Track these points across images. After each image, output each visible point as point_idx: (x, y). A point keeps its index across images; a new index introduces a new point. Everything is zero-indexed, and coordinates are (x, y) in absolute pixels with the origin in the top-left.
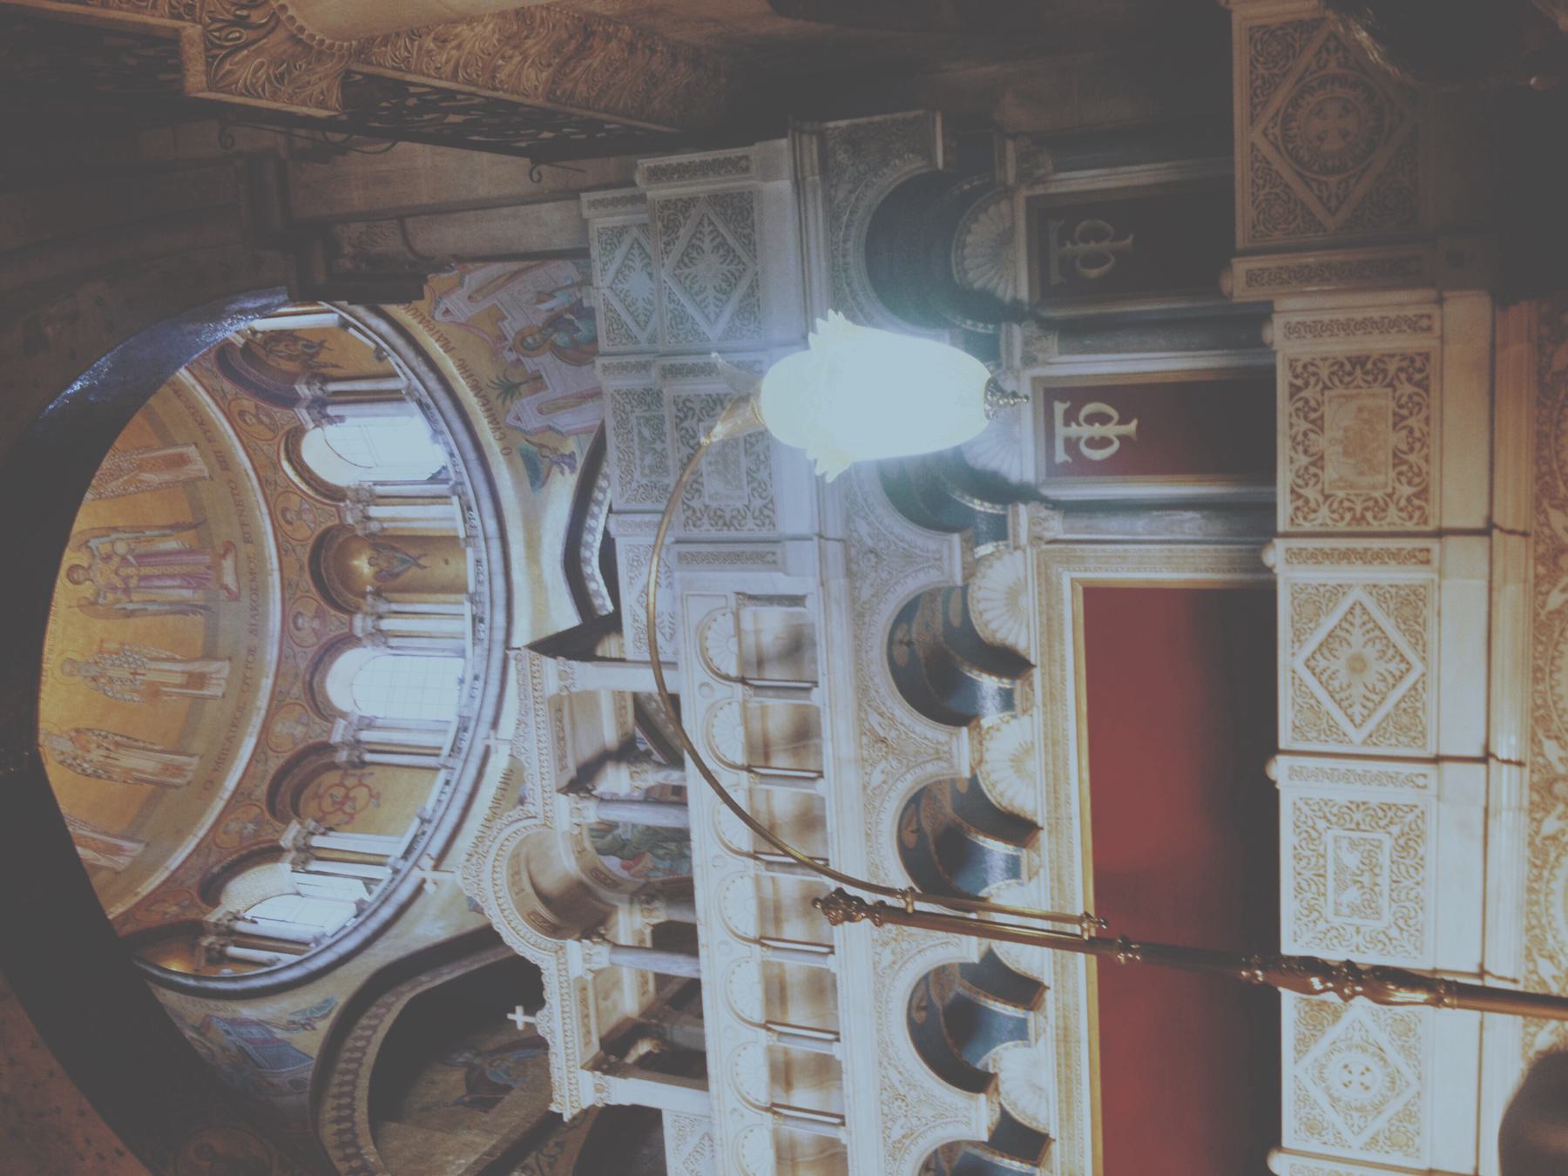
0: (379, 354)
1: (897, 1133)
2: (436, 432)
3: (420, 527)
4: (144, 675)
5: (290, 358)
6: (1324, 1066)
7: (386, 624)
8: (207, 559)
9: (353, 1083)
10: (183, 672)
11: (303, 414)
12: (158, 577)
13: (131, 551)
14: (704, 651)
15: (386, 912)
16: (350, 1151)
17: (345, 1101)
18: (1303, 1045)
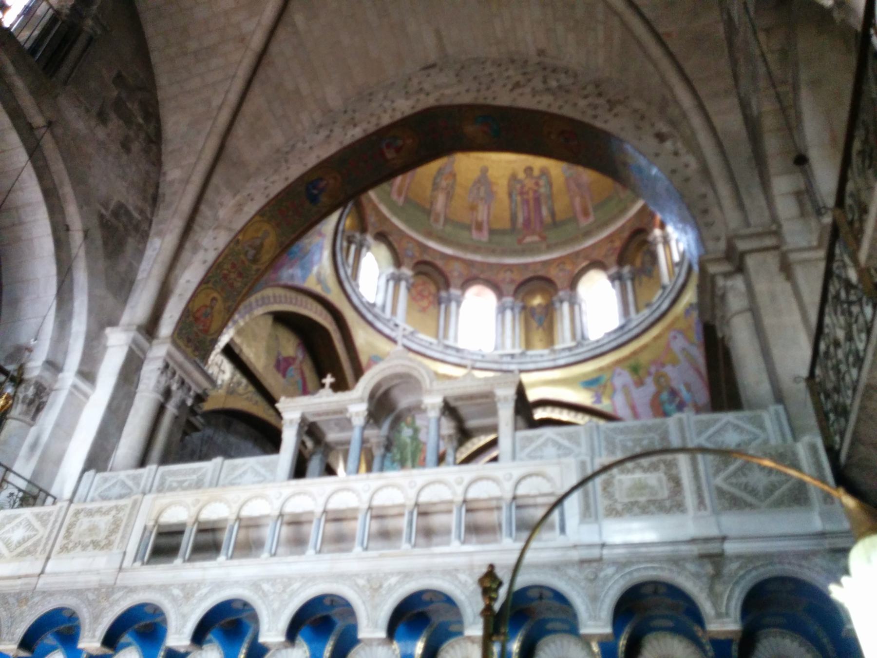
0: (648, 305)
1: (266, 587)
2: (609, 334)
3: (558, 327)
5: (643, 263)
7: (509, 314)
9: (291, 303)
11: (614, 270)
14: (530, 475)
15: (370, 317)
16: (260, 302)
17: (283, 299)
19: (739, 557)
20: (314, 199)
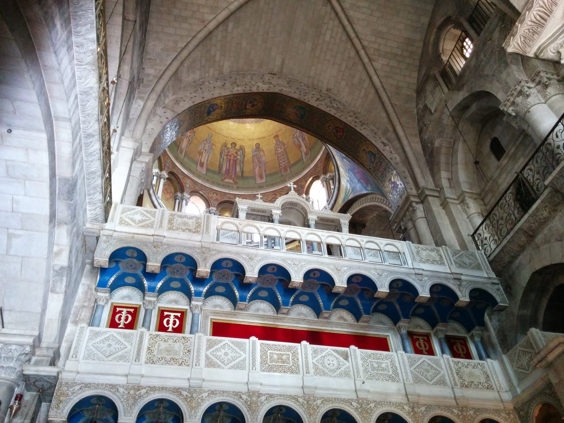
1: (289, 262)
6: (332, 356)
8: (233, 176)
13: (237, 159)
18: (337, 352)
19: (466, 281)
20: (209, 113)
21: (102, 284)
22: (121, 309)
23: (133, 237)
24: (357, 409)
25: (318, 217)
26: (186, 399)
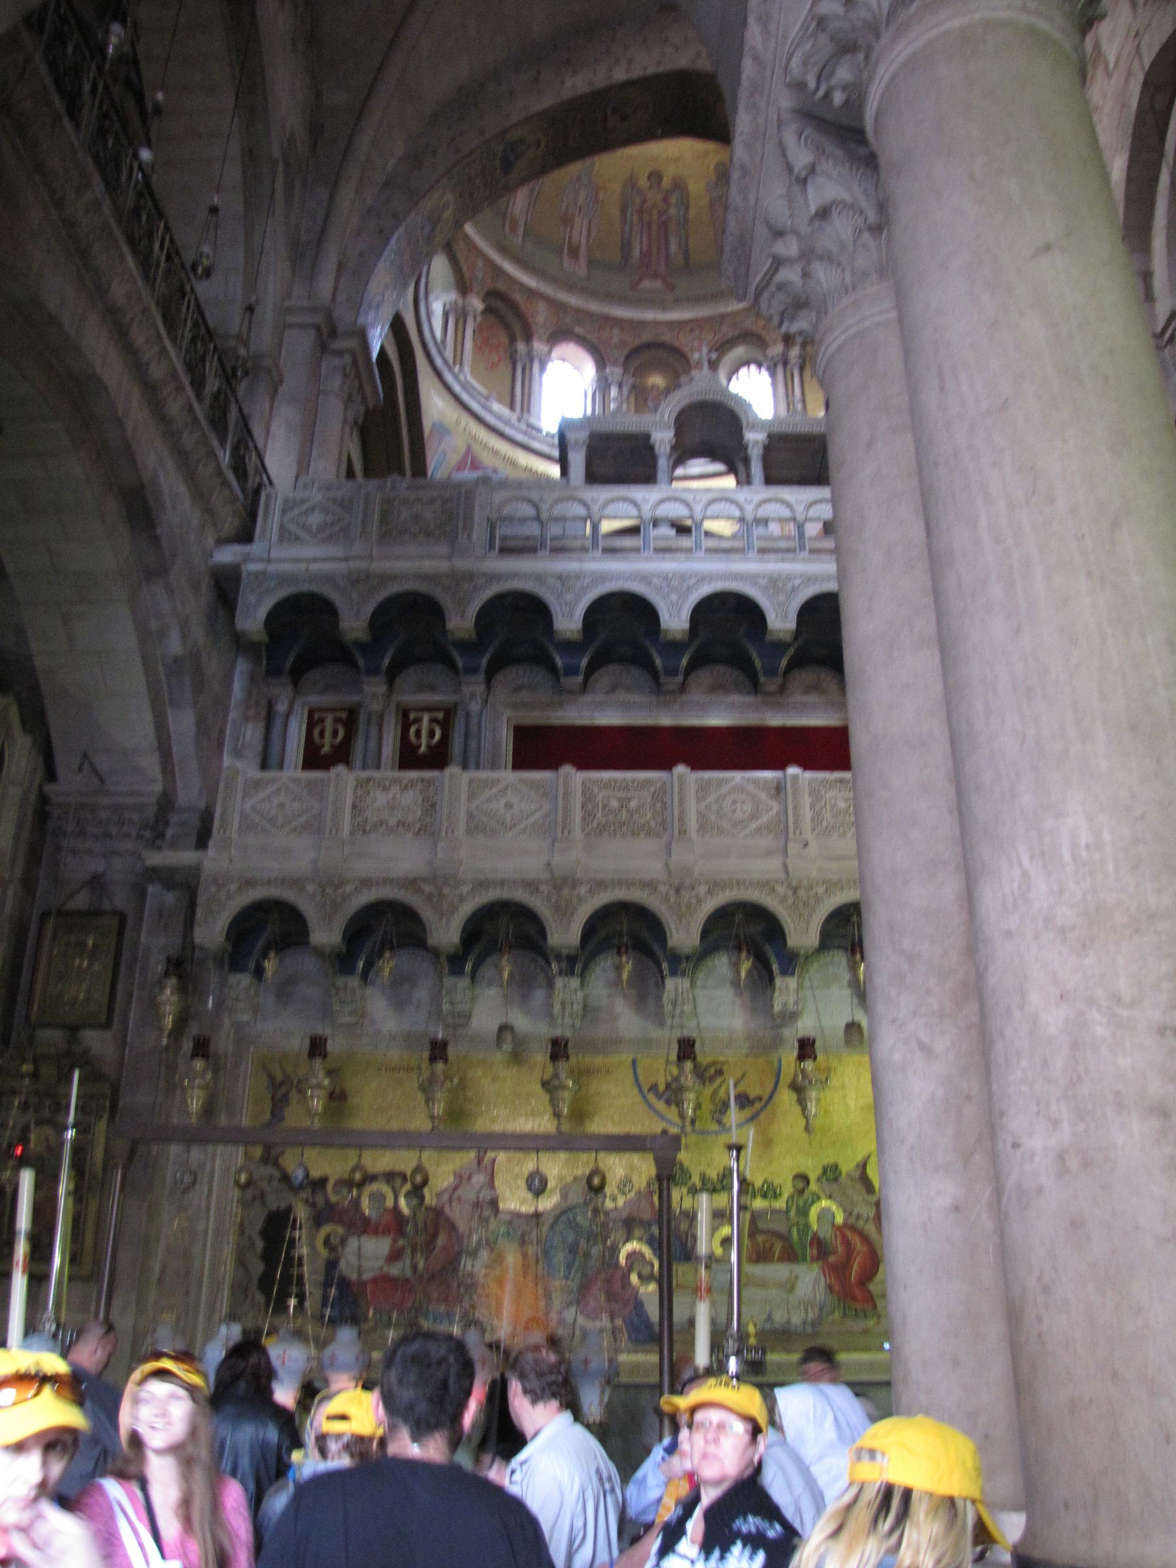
4: (579, 215)
7: (614, 392)
10: (580, 242)
12: (650, 234)
21: (274, 671)
22: (324, 715)
23: (307, 570)
24: (784, 899)
25: (770, 436)
26: (429, 898)
